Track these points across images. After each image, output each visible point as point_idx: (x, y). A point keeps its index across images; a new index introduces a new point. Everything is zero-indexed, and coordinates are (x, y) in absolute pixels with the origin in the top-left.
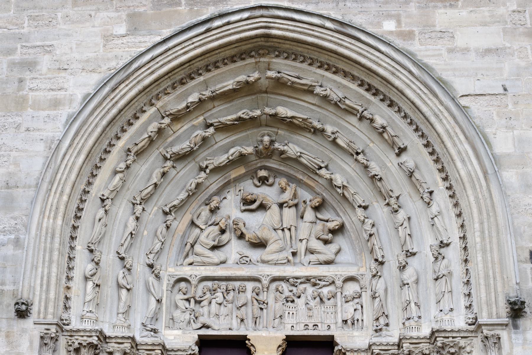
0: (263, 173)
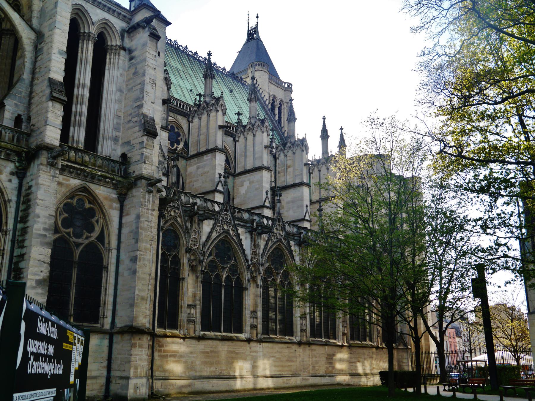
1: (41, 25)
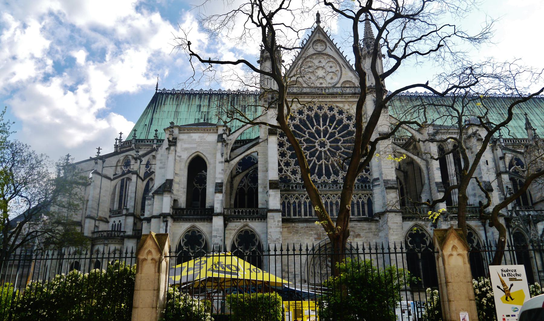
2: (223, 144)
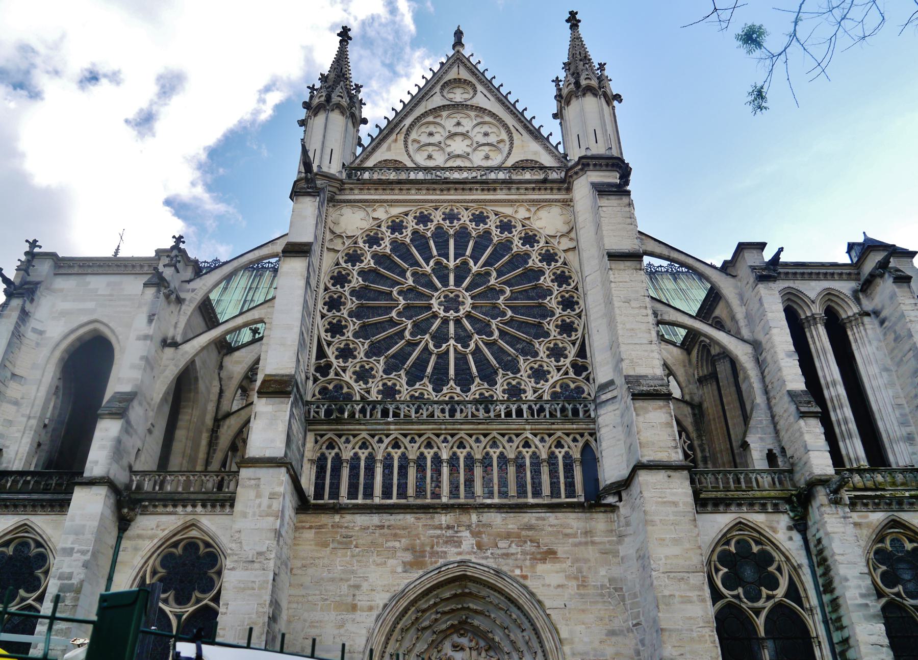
0: (462, 632)
1: (753, 332)
2: (159, 291)
